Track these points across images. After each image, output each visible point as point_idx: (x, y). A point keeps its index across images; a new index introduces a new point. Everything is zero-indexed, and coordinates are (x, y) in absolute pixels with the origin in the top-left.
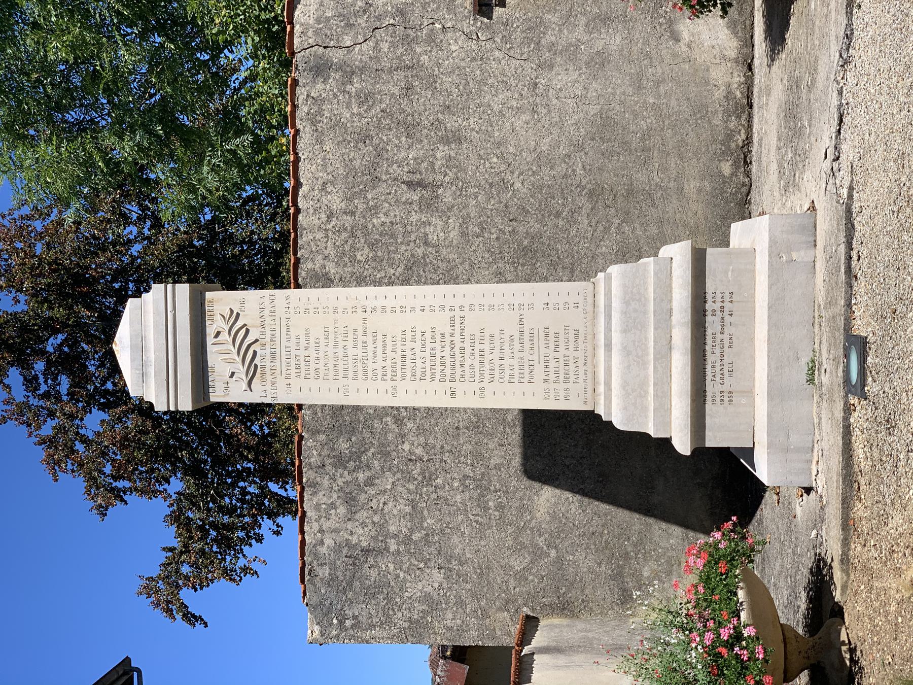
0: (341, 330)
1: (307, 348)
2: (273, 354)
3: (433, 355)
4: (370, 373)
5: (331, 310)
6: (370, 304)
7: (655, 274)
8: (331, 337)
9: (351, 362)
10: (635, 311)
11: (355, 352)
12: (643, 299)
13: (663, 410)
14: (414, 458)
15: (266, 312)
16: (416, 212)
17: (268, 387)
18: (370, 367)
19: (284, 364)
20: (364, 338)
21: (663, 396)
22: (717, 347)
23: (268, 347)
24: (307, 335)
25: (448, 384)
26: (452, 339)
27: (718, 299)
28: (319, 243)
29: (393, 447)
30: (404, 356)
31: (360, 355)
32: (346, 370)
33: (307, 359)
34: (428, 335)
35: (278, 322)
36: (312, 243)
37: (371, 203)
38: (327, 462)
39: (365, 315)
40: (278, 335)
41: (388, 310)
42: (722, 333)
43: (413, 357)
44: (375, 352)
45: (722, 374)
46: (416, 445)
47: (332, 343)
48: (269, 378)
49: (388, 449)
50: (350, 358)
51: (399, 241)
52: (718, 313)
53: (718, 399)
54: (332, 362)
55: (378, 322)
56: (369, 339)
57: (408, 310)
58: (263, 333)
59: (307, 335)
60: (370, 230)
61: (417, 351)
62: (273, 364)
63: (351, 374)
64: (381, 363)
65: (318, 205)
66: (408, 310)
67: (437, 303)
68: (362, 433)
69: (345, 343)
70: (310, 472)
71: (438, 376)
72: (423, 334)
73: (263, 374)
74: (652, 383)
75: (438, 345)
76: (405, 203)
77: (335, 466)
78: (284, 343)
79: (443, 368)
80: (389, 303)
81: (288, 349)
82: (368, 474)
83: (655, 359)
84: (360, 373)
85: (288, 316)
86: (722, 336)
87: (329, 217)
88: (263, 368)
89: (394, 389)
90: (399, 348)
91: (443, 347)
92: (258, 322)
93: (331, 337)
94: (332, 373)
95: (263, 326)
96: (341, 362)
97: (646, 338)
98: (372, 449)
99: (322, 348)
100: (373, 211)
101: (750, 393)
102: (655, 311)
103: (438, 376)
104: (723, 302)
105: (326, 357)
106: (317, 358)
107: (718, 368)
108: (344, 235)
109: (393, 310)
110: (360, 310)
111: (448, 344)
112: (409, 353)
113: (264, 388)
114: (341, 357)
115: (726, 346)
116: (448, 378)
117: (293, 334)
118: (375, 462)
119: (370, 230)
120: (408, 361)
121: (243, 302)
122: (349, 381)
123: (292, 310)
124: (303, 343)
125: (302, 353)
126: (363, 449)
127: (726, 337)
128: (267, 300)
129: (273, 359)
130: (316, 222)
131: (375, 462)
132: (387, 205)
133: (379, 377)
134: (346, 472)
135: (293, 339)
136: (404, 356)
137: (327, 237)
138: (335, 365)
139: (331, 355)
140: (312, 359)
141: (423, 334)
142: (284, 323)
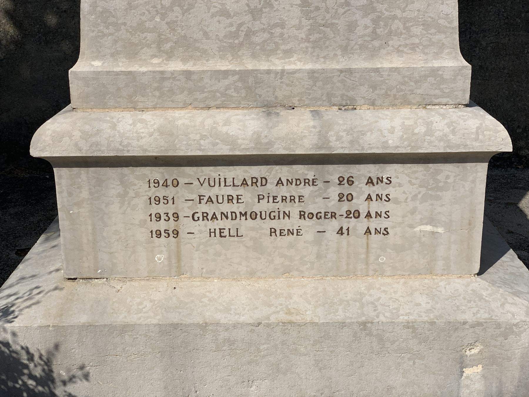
7: (434, 72)
10: (352, 27)
12: (376, 43)
13: (131, 93)
21: (163, 91)
22: (271, 206)
27: (375, 207)
42: (302, 215)
45: (214, 217)
52: (345, 206)
53: (161, 209)
74: (189, 66)
83: (243, 75)
86: (295, 214)
97: (288, 53)
101: (178, 267)
102: (350, 71)
104: (369, 215)
107: (226, 208)
115: (275, 224)
127: (294, 222)
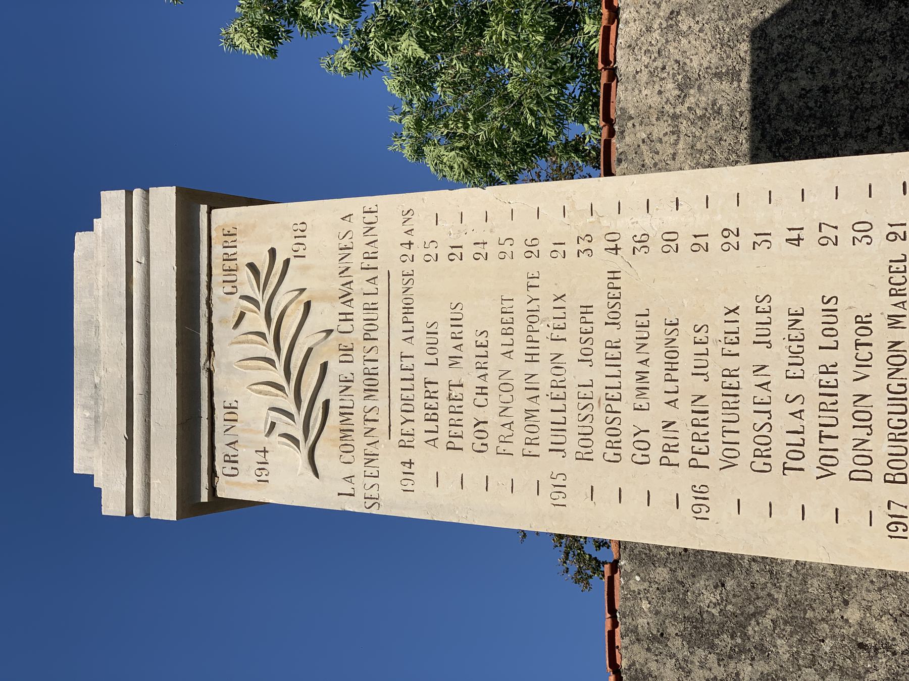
0: (546, 309)
1: (454, 361)
2: (371, 375)
3: (828, 390)
4: (627, 440)
5: (519, 249)
6: (628, 227)
8: (521, 327)
9: (572, 404)
11: (584, 373)
14: (870, 642)
15: (356, 259)
16: (883, 59)
17: (358, 467)
18: (629, 420)
19: (397, 405)
20: (612, 333)
23: (358, 355)
24: (456, 322)
25: (880, 491)
26: (897, 335)
28: (658, 146)
29: (821, 612)
30: (731, 391)
31: (601, 382)
32: (559, 427)
33: (456, 391)
34: (812, 323)
35: (382, 285)
36: (644, 147)
37: (777, 48)
38: (671, 630)
39: (615, 262)
40: (382, 322)
41: (685, 243)
43: (762, 394)
44: (642, 376)
46: (876, 609)
47: (520, 348)
48: (360, 442)
49: (810, 614)
50: (572, 392)
51: (841, 131)
54: (520, 404)
55: (658, 285)
56: (627, 334)
57: (746, 240)
58: (346, 317)
59: (456, 322)
60: (772, 111)
61: (776, 374)
62: (370, 404)
63: (572, 443)
64: (660, 411)
65: (659, 64)
66: (746, 240)
67: (845, 213)
68: (748, 572)
69: (557, 347)
70: (636, 647)
71: (846, 461)
72: (796, 318)
73: (346, 433)
75: (845, 357)
76: (857, 41)
77: (692, 645)
78: (398, 346)
79: (862, 433)
80: (687, 222)
81: (407, 363)
82: (762, 667)
84: (600, 439)
85: (408, 267)
87: (683, 88)
88: (346, 413)
89: (701, 494)
90: (717, 364)
91: (864, 363)
92: (336, 285)
93: (521, 327)
94: (520, 435)
95: (346, 297)
96: (544, 404)
98: (772, 612)
99: (496, 363)
100: (781, 67)
103: (846, 461)
105: (506, 387)
106: (482, 391)
108: (716, 125)
109: (700, 246)
110: (599, 246)
111: (880, 353)
112: (748, 382)
113: (347, 470)
114: (545, 387)
116: (879, 469)
117: (419, 319)
118: (779, 642)
119: (772, 111)
120: (746, 408)
121: (301, 232)
122: (569, 464)
123: (418, 251)
124: (446, 345)
125: (443, 375)
126: (751, 609)
128: (358, 226)
129: (371, 391)
130: (654, 100)
131: (779, 642)
132: (814, 49)
133: (655, 453)
134: (713, 658)
135: (420, 334)
136: (731, 391)
137: (676, 132)
138: (530, 414)
139: (519, 383)
140: (469, 393)
141: (796, 318)
142: (397, 287)
